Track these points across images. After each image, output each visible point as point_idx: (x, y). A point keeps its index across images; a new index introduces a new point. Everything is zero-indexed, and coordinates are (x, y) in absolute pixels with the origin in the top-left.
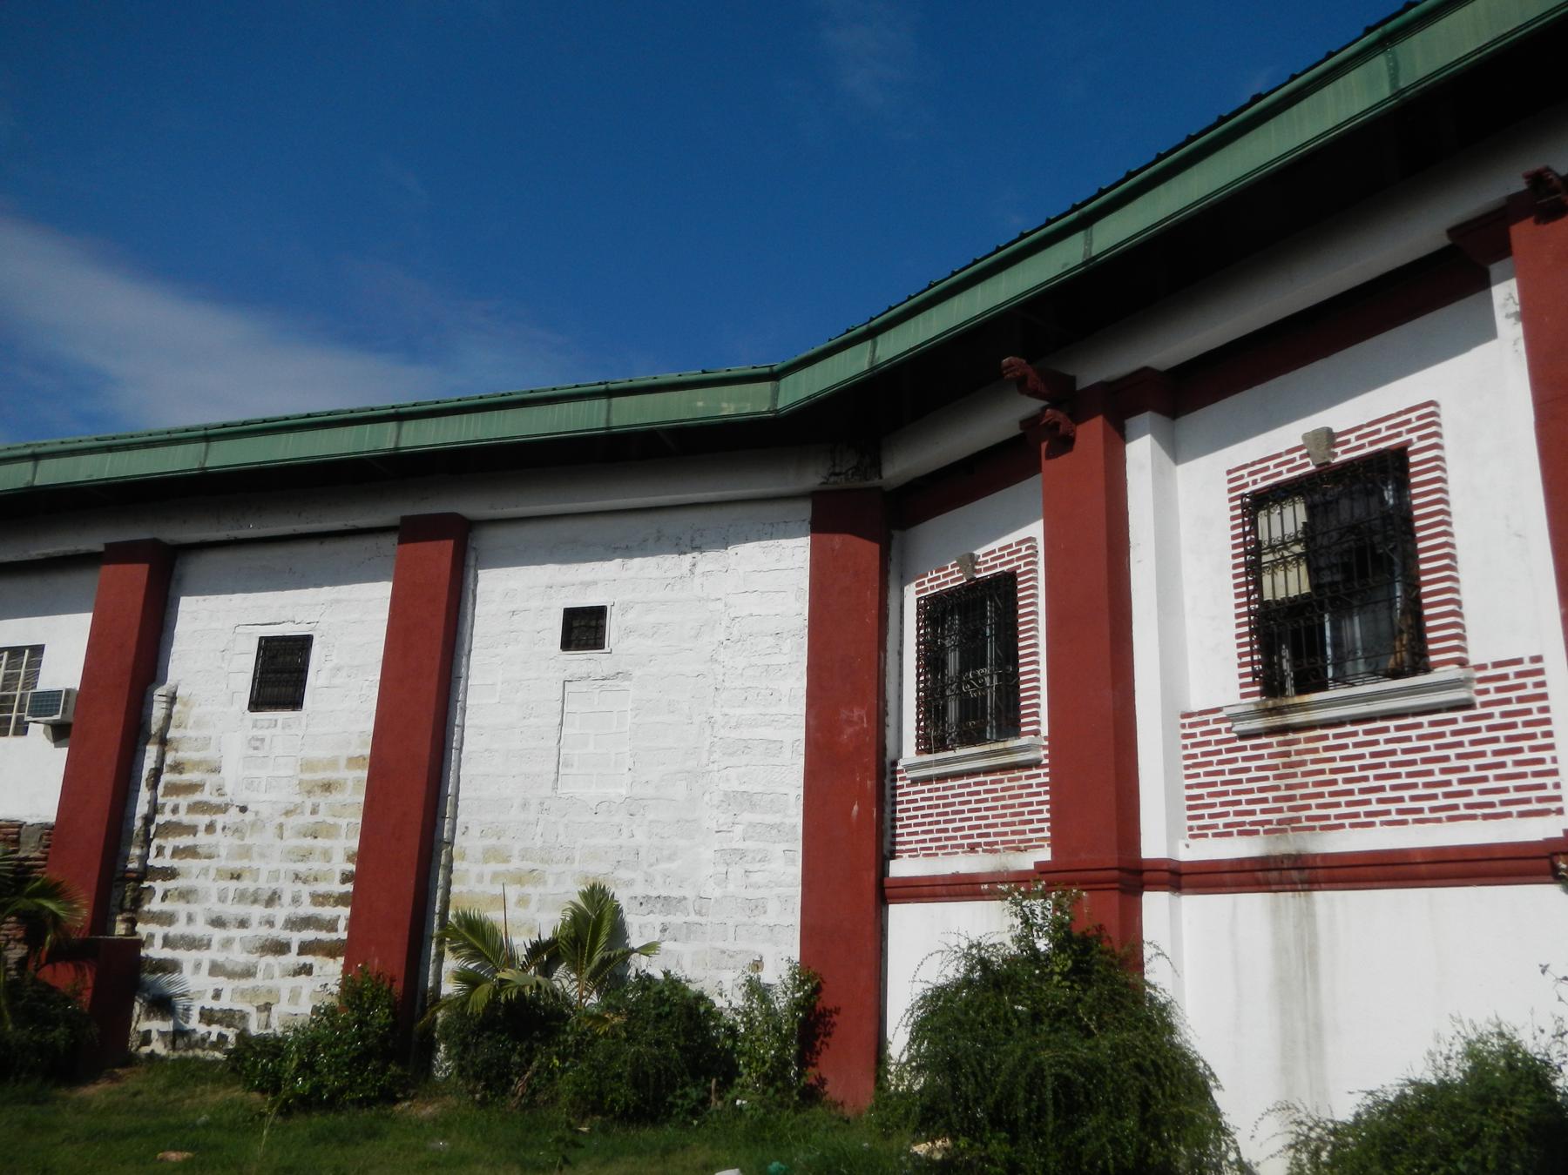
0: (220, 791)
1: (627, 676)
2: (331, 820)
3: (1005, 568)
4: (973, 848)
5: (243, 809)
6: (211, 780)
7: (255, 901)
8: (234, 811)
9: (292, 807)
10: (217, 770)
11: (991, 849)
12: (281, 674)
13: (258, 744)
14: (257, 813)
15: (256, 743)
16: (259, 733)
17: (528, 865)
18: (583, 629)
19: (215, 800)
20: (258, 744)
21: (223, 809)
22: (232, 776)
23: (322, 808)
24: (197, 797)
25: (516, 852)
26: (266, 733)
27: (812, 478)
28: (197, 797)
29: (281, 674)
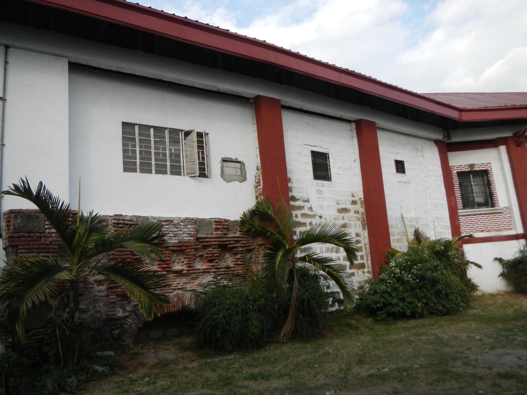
0: (311, 209)
1: (408, 182)
2: (349, 222)
3: (483, 169)
4: (482, 231)
5: (321, 217)
6: (307, 205)
7: (332, 252)
8: (318, 218)
9: (336, 217)
10: (308, 201)
11: (489, 231)
12: (321, 166)
13: (320, 192)
14: (326, 219)
15: (320, 192)
16: (320, 188)
17: (399, 237)
18: (400, 167)
19: (309, 213)
20: (320, 192)
21: (313, 216)
22: (314, 203)
23: (345, 218)
24: (303, 212)
25: (396, 233)
26: (322, 189)
27: (440, 137)
28: (303, 212)
29: (321, 166)
